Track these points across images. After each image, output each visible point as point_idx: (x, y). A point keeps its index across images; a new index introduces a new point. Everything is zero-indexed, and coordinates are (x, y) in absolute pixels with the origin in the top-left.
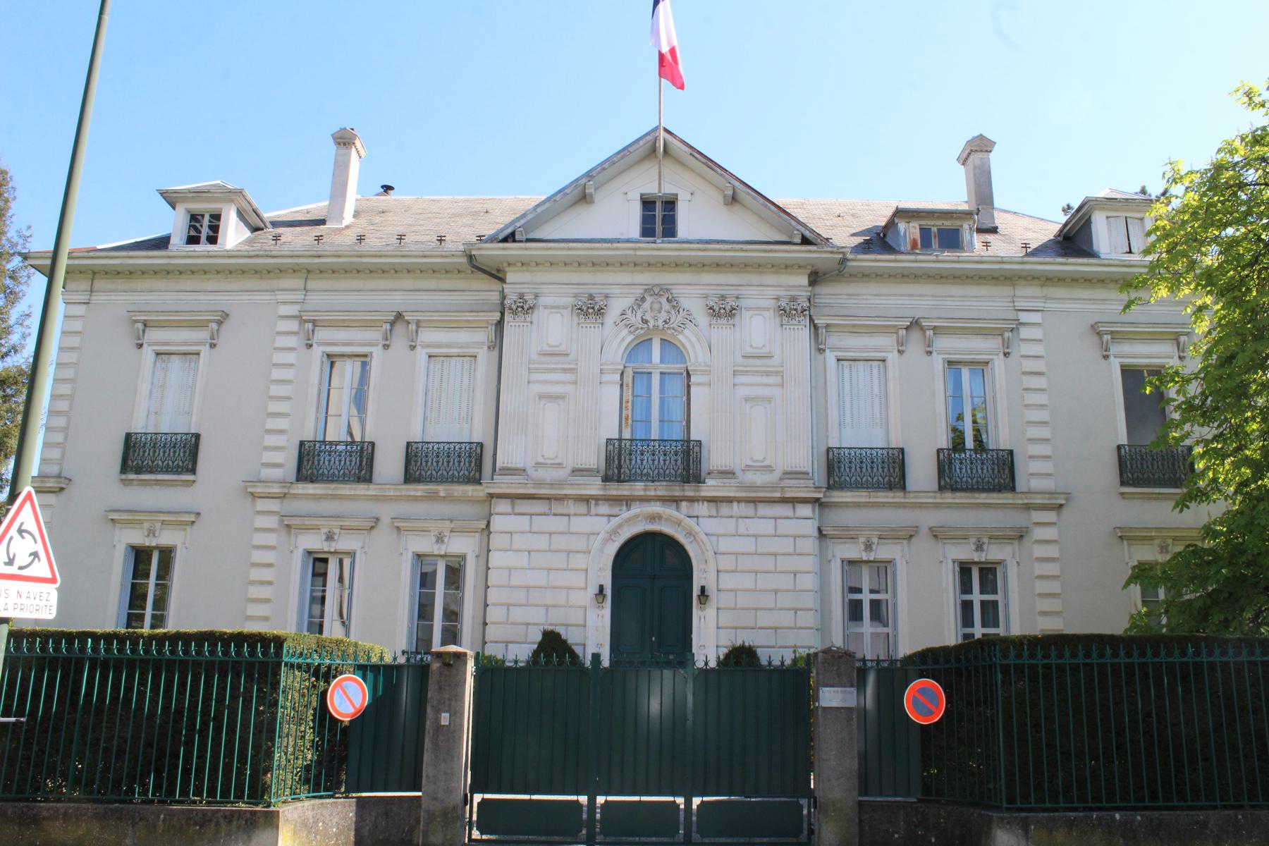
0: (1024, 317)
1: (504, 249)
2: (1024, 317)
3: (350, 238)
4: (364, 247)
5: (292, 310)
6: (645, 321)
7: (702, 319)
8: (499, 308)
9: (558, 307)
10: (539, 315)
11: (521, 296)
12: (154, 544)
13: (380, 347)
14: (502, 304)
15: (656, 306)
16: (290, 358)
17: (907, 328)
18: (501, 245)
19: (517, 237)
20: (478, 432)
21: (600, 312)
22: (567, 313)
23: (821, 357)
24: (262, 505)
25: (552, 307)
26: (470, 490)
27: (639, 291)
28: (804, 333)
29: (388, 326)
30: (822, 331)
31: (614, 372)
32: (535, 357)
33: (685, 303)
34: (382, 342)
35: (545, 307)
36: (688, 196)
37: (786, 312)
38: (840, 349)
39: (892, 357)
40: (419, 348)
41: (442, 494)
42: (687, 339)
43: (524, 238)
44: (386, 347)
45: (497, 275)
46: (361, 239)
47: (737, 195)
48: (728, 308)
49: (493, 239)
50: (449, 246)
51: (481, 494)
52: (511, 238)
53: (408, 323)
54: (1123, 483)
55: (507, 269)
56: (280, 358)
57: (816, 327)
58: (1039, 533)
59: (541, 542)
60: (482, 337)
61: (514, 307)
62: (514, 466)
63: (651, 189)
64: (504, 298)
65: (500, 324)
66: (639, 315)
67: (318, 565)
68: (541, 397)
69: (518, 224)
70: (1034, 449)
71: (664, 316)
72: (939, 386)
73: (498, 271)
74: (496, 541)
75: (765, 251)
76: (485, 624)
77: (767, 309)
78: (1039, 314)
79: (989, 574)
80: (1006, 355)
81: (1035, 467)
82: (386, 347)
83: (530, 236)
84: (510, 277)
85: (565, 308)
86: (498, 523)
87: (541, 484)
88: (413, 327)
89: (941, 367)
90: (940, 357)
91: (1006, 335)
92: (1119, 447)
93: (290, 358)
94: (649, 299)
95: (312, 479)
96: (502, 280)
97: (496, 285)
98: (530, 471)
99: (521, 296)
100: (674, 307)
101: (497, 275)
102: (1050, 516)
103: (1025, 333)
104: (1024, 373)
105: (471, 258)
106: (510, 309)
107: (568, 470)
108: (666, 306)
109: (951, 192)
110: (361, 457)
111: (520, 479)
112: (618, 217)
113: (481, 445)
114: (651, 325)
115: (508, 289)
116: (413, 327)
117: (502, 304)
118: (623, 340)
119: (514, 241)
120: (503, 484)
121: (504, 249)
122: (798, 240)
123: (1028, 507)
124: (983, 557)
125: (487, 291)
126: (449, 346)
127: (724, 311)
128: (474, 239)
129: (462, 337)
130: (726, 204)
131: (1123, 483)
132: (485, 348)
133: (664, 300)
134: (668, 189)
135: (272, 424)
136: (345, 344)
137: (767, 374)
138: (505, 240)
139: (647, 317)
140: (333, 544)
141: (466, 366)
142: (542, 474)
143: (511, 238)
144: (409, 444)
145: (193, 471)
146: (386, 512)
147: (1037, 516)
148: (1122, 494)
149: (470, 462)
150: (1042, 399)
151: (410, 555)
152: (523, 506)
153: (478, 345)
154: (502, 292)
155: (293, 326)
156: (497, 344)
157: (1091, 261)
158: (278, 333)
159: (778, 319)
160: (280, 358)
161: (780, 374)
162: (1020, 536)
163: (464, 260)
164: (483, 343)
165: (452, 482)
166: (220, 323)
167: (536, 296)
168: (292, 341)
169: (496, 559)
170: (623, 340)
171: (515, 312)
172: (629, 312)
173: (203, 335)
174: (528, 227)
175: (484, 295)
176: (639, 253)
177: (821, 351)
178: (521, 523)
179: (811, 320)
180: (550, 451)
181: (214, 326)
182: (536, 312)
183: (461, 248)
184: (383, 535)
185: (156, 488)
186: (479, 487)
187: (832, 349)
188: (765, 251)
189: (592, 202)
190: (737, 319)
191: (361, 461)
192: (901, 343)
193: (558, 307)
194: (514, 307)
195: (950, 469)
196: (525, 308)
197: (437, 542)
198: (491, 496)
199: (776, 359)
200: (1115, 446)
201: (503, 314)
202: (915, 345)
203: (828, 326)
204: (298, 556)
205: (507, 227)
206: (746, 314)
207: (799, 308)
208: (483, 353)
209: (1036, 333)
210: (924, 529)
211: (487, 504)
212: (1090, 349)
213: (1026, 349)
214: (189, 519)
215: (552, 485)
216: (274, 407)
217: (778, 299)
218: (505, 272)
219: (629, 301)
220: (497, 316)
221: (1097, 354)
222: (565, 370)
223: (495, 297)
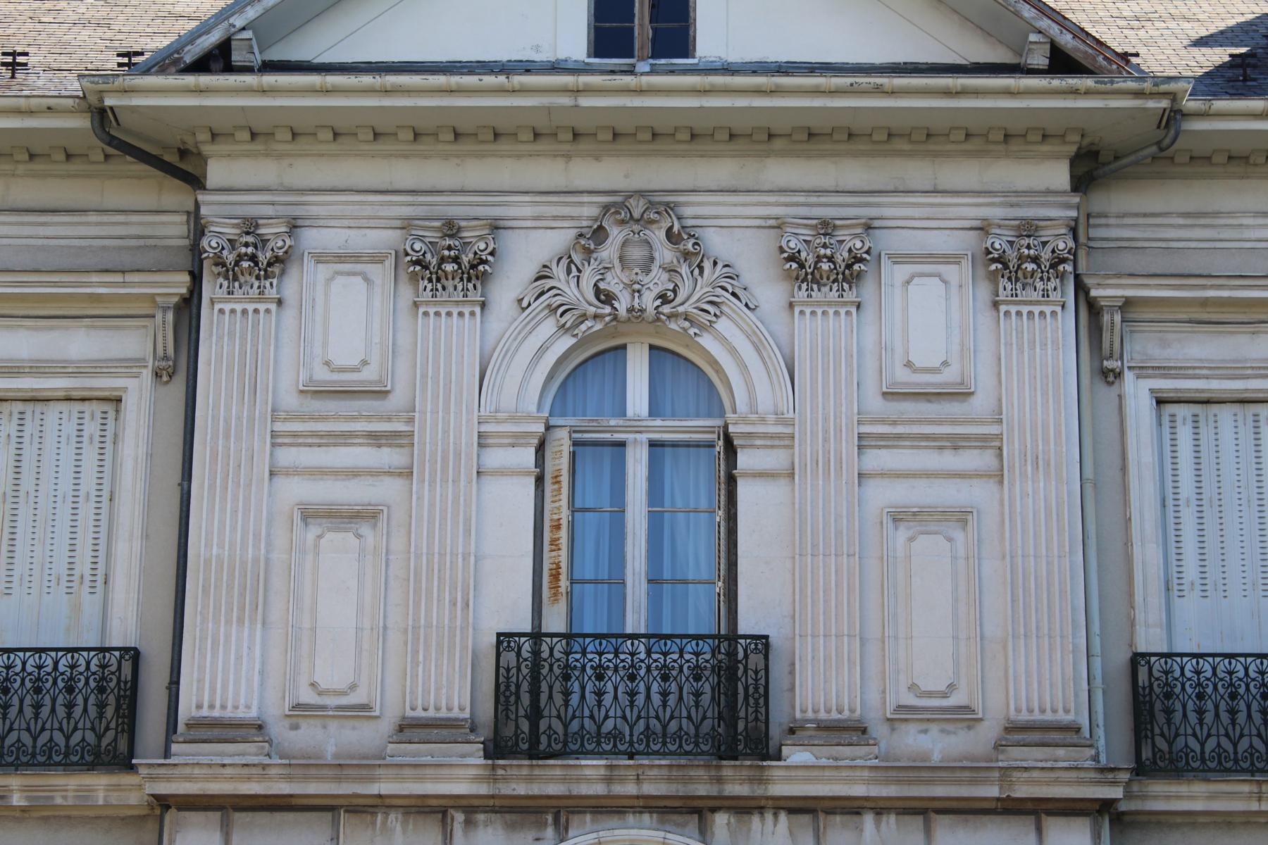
1: (199, 91)
8: (185, 260)
9: (356, 258)
11: (250, 226)
14: (196, 250)
18: (190, 80)
19: (237, 57)
20: (125, 620)
21: (477, 272)
22: (382, 274)
23: (1107, 395)
25: (340, 258)
26: (100, 787)
31: (516, 440)
32: (290, 400)
35: (320, 258)
37: (1008, 266)
38: (1164, 371)
41: (17, 800)
43: (258, 58)
45: (181, 165)
49: (167, 62)
50: (38, 82)
51: (134, 799)
52: (218, 59)
55: (207, 149)
60: (135, 342)
61: (230, 257)
62: (229, 714)
64: (198, 229)
65: (188, 310)
68: (309, 514)
69: (239, 21)
73: (183, 153)
75: (948, 93)
83: (275, 55)
84: (216, 173)
85: (377, 259)
87: (307, 765)
96: (195, 181)
97: (176, 196)
98: (278, 729)
99: (250, 226)
101: (181, 165)
105: (102, 116)
107: (386, 726)
111: (249, 752)
113: (133, 655)
115: (210, 205)
117: (196, 250)
119: (229, 68)
120: (198, 770)
121: (199, 91)
122: (1040, 59)
125: (144, 212)
126: (37, 368)
128: (112, 62)
129: (79, 343)
132: (147, 374)
138: (201, 65)
141: (92, 428)
142: (308, 736)
143: (218, 59)
149: (101, 706)
153: (129, 365)
154: (195, 215)
156: (181, 363)
159: (984, 291)
161: (992, 443)
163: (82, 123)
164: (140, 362)
165: (49, 765)
167: (294, 226)
171: (231, 273)
174: (264, 29)
175: (136, 225)
176: (585, 102)
177: (1110, 376)
180: (333, 670)
182: (293, 271)
183: (74, 86)
186: (127, 779)
187: (1142, 371)
188: (948, 93)
193: (356, 258)
194: (230, 257)
196: (261, 261)
198: (164, 803)
199: (981, 404)
201: (196, 278)
203: (1128, 304)
205: (205, 28)
207: (1046, 255)
208: (138, 392)
211: (152, 826)
215: (340, 768)
217: (983, 229)
218: (203, 160)
220: (179, 283)
222: (376, 439)
223: (174, 229)
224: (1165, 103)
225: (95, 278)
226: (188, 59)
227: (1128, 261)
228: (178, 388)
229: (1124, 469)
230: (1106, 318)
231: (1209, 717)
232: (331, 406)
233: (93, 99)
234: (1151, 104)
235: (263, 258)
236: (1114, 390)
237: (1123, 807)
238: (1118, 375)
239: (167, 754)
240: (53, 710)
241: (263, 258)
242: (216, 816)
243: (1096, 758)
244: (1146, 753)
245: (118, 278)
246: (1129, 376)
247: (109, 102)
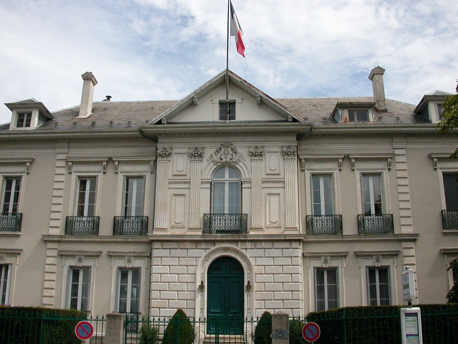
0: (397, 152)
2: (397, 152)
3: (89, 123)
4: (94, 129)
5: (63, 157)
6: (222, 159)
7: (248, 159)
9: (182, 154)
10: (174, 158)
11: (165, 149)
12: (3, 263)
13: (102, 172)
14: (156, 152)
15: (226, 152)
16: (62, 178)
17: (343, 159)
19: (162, 122)
21: (200, 156)
22: (186, 156)
23: (303, 174)
24: (50, 245)
25: (179, 154)
27: (218, 145)
28: (295, 163)
29: (105, 163)
30: (303, 161)
31: (207, 182)
32: (171, 177)
33: (239, 150)
34: (103, 171)
35: (176, 154)
36: (241, 101)
37: (285, 154)
38: (312, 170)
39: (336, 173)
40: (119, 173)
42: (240, 166)
44: (104, 173)
46: (94, 123)
47: (262, 101)
48: (259, 152)
53: (114, 162)
54: (444, 228)
55: (158, 137)
56: (57, 178)
57: (300, 160)
58: (405, 252)
59: (175, 262)
63: (223, 98)
65: (155, 161)
66: (219, 156)
67: (75, 272)
68: (174, 195)
69: (163, 117)
70: (403, 213)
71: (230, 157)
72: (358, 185)
73: (155, 137)
74: (155, 261)
75: (275, 126)
76: (150, 299)
77: (277, 152)
78: (404, 150)
79: (384, 272)
80: (389, 170)
81: (404, 221)
82: (104, 173)
84: (159, 141)
85: (185, 154)
86: (155, 253)
88: (116, 163)
89: (359, 177)
90: (359, 171)
91: (389, 160)
92: (442, 211)
93: (62, 178)
94: (223, 149)
95: (72, 234)
100: (234, 152)
102: (411, 244)
103: (398, 159)
104: (398, 178)
105: (142, 132)
106: (160, 154)
108: (231, 152)
109: (363, 92)
110: (94, 223)
112: (209, 114)
114: (224, 161)
116: (116, 163)
118: (211, 168)
122: (291, 120)
123: (401, 241)
124: (379, 265)
127: (257, 155)
130: (258, 104)
131: (444, 228)
132: (149, 172)
133: (230, 149)
134: (231, 98)
135: (54, 208)
136: (86, 172)
137: (278, 182)
139: (222, 157)
140: (81, 263)
144: (115, 217)
145: (20, 230)
146: (105, 249)
147: (405, 244)
148: (444, 233)
150: (407, 189)
151: (116, 268)
152: (166, 245)
155: (63, 164)
156: (154, 172)
157: (426, 125)
158: (57, 167)
159: (282, 158)
160: (57, 178)
161: (284, 182)
162: (395, 254)
163: (139, 133)
166: (31, 163)
167: (172, 149)
168: (63, 171)
169: (155, 269)
170: (211, 168)
172: (214, 155)
173: (22, 169)
176: (218, 128)
177: (303, 171)
178: (166, 252)
179: (298, 157)
181: (28, 164)
182: (172, 156)
184: (103, 259)
185: (4, 238)
187: (308, 170)
188: (275, 126)
189: (197, 105)
190: (263, 158)
191: (94, 225)
192: (340, 165)
193: (182, 154)
194: (162, 154)
195: (364, 224)
197: (128, 262)
199: (282, 176)
200: (441, 211)
201: (157, 157)
202: (346, 167)
203: (306, 159)
204: (66, 268)
206: (268, 155)
207: (292, 151)
209: (403, 159)
210: (351, 253)
212: (427, 166)
213: (399, 166)
214: (16, 253)
216: (55, 200)
217: (282, 147)
218: (158, 139)
219: (214, 150)
221: (431, 168)
222: (185, 183)
224: (310, 127)
225: (141, 157)
226: (155, 122)
227: (306, 152)
228: (154, 175)
229: (305, 185)
230: (302, 161)
231: (318, 225)
232: (178, 178)
233: (140, 129)
234: (309, 127)
235: (167, 154)
236: (304, 172)
237: (304, 240)
238: (304, 170)
239: (152, 233)
240: (135, 226)
241: (167, 154)
242: (160, 243)
243: (300, 232)
244: (308, 232)
245: (145, 157)
246: (306, 170)
247: (142, 130)
